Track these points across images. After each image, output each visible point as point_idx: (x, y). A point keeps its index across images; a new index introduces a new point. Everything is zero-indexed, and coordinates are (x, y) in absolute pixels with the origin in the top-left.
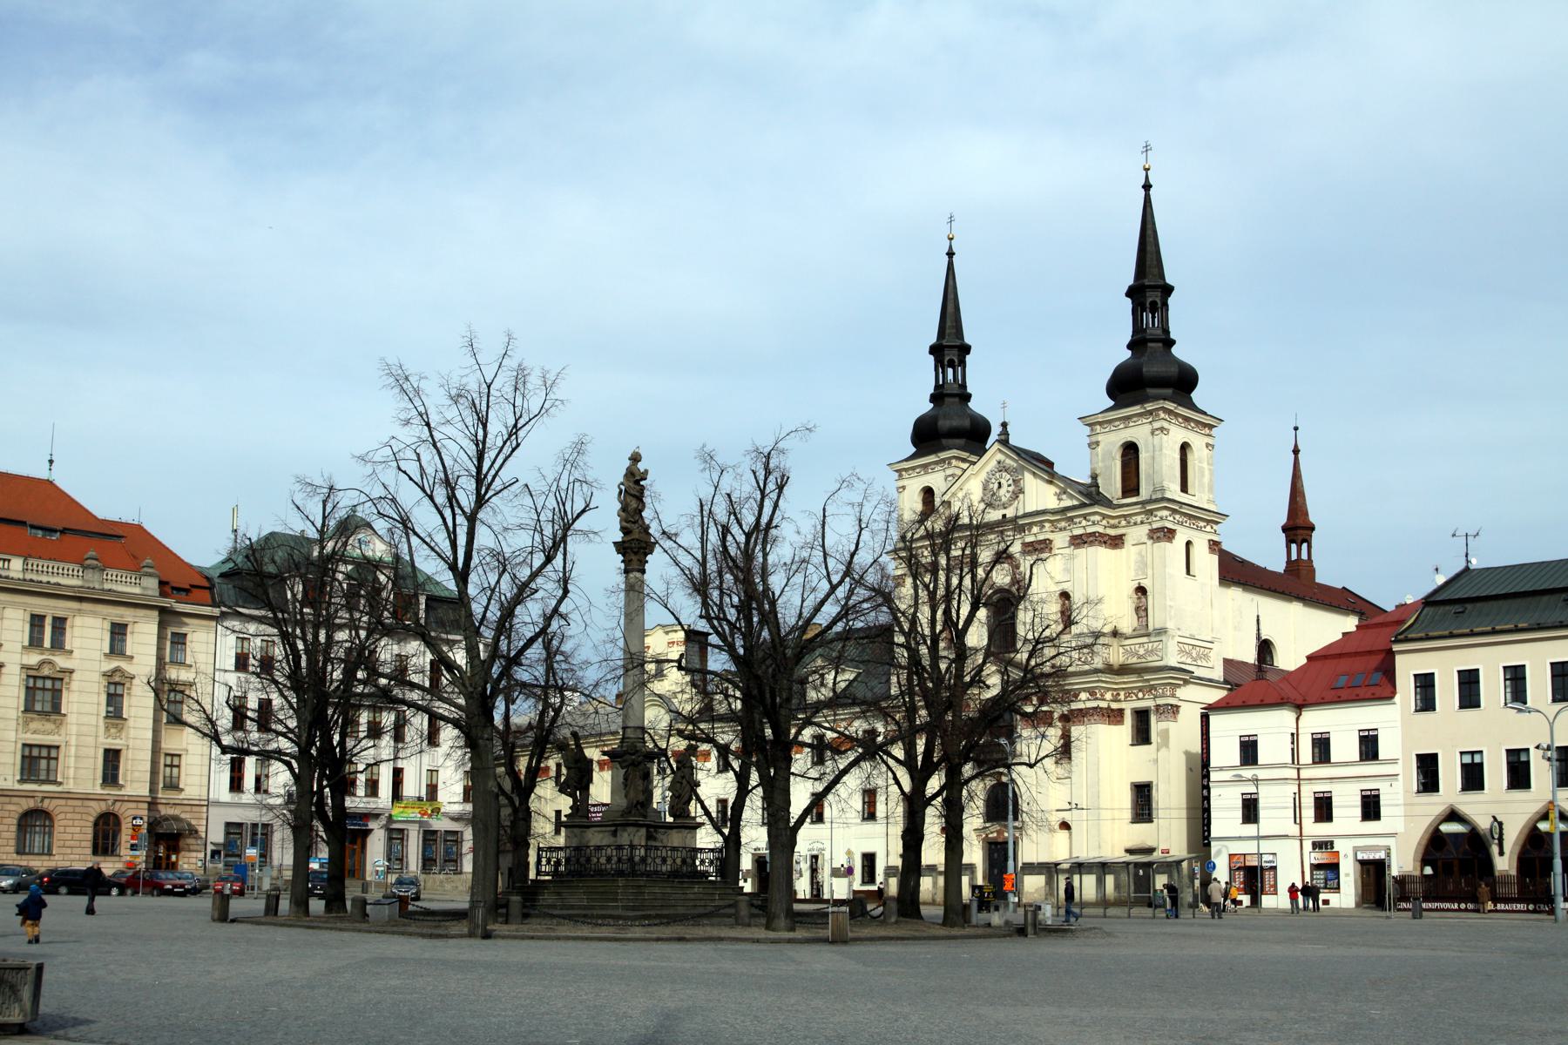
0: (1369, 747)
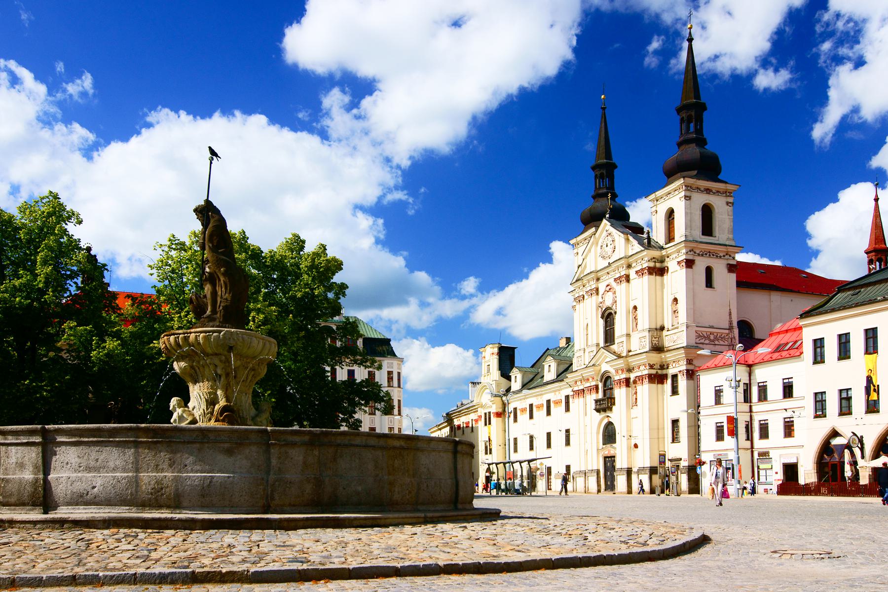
0: (788, 390)
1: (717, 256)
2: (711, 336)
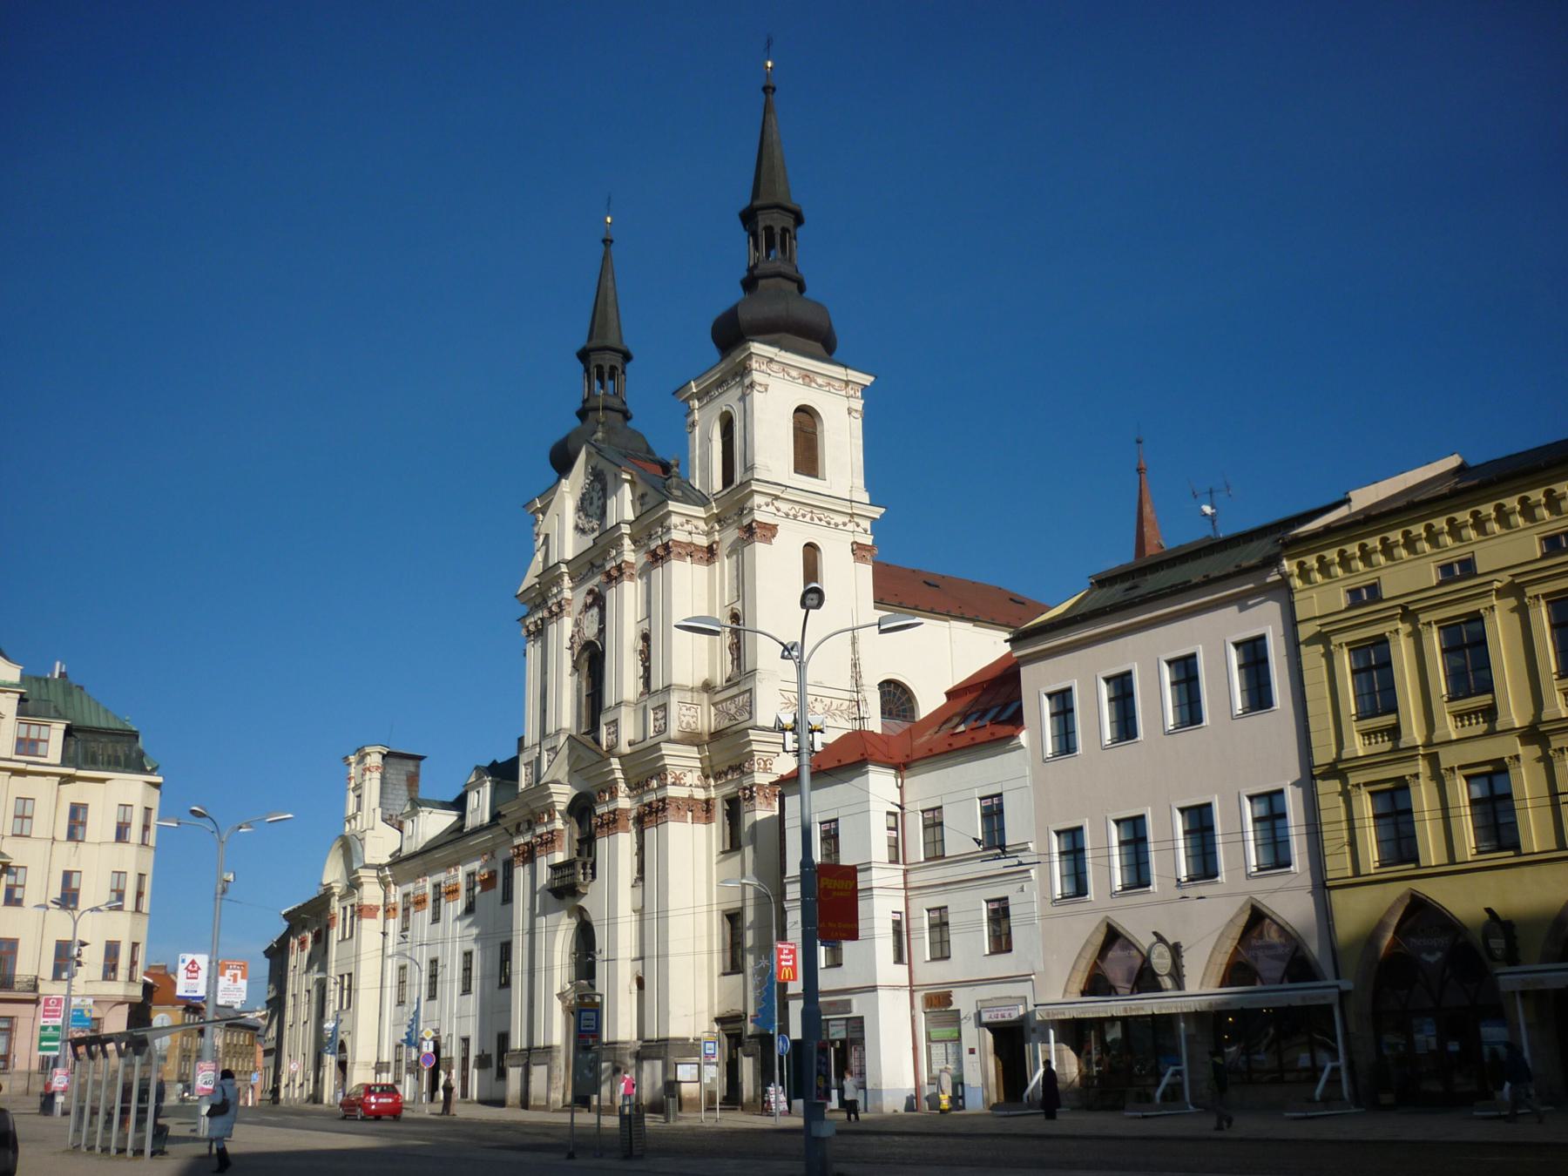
1: (829, 523)
2: (816, 704)
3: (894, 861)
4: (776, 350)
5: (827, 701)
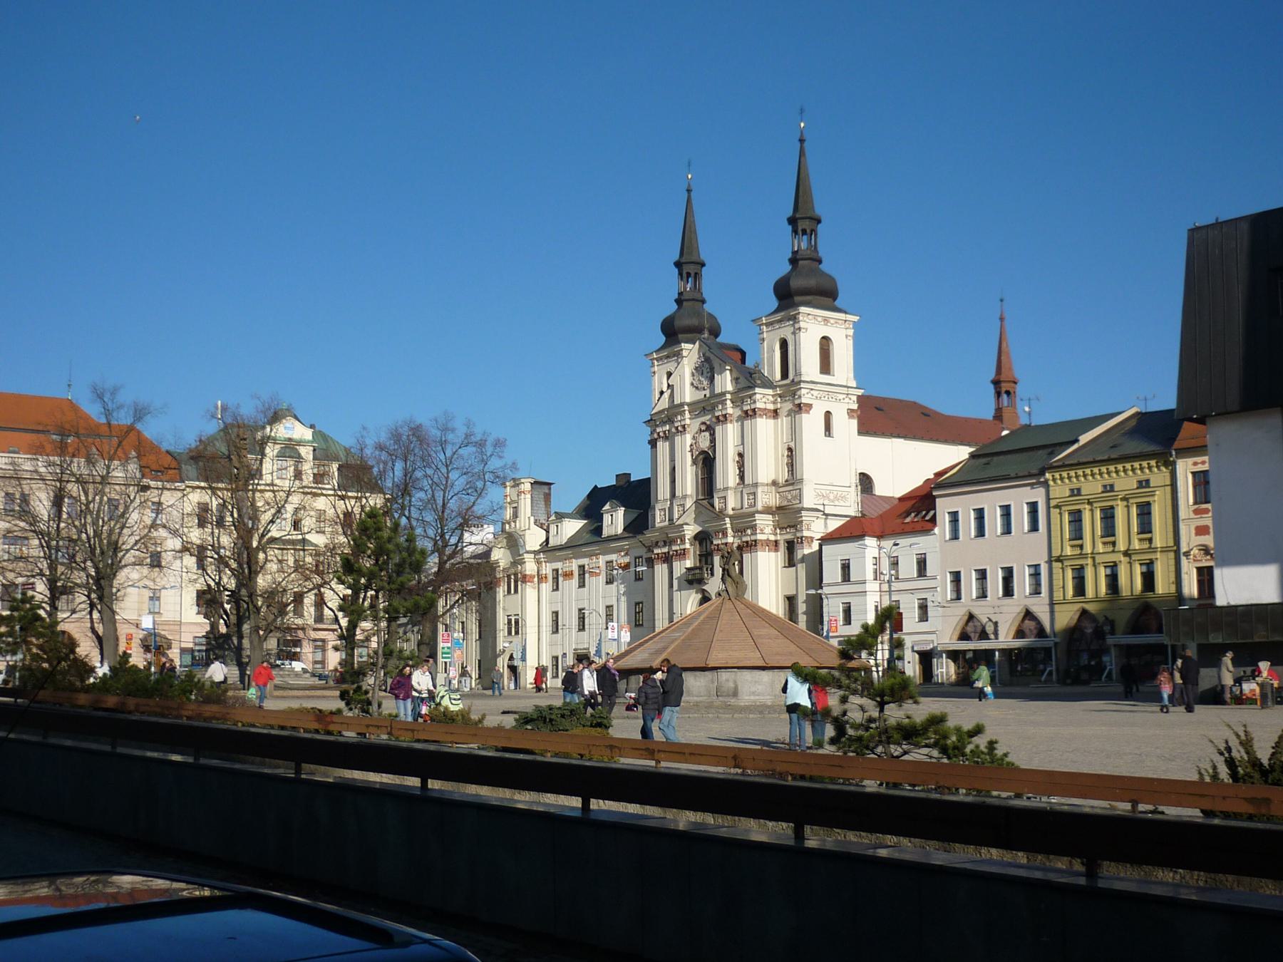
2: (831, 495)
3: (876, 579)
4: (811, 309)
5: (835, 493)
